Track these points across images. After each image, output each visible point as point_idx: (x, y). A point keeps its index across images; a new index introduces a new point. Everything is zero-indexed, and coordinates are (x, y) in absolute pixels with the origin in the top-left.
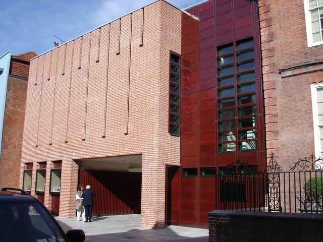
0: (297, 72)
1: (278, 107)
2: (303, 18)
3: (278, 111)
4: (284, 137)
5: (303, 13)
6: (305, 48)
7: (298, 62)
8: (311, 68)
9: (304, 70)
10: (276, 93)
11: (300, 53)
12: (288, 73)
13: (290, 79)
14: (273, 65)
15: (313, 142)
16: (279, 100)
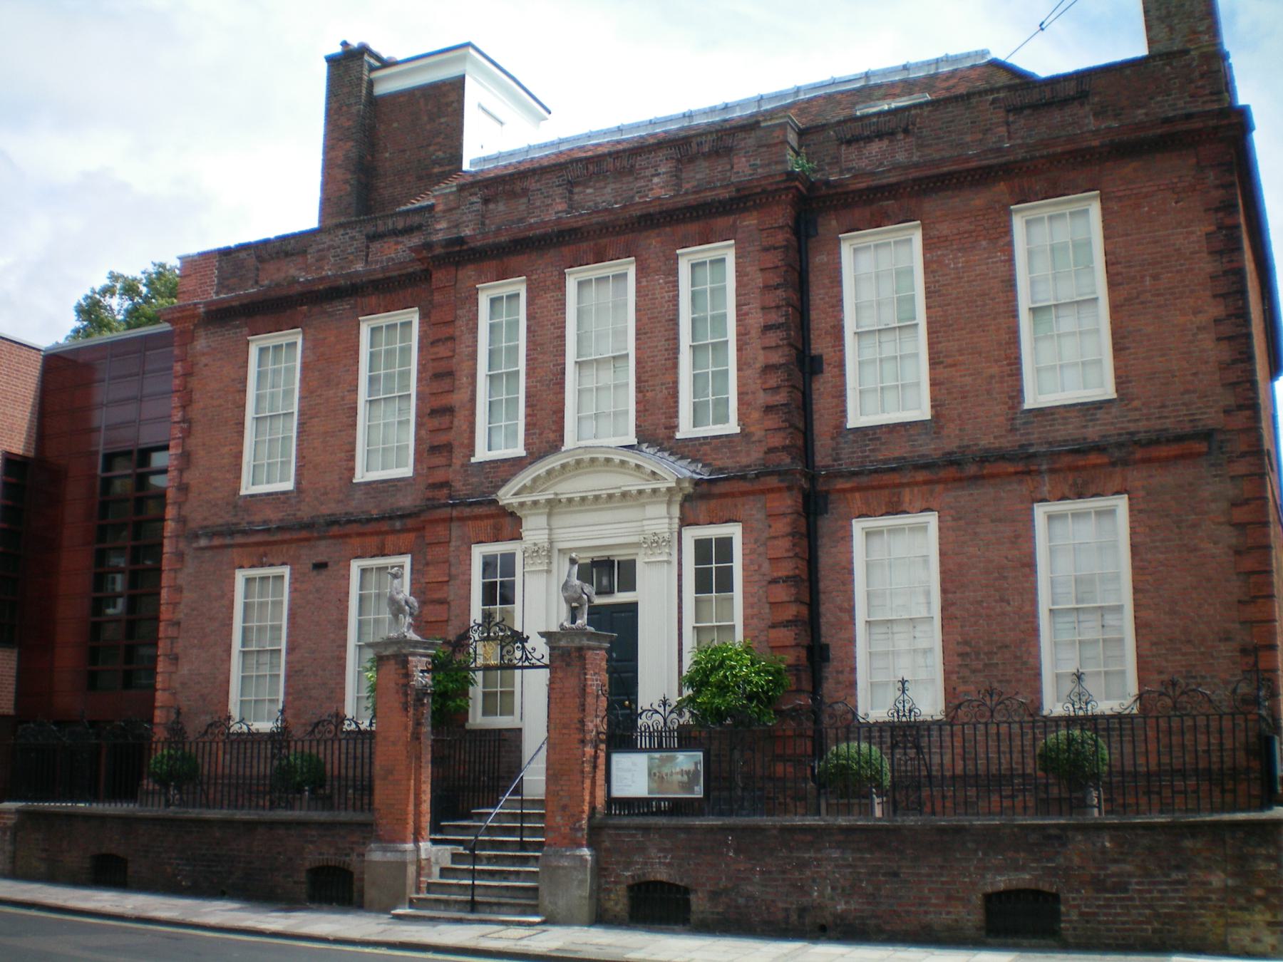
0: (217, 542)
1: (182, 606)
2: (241, 433)
3: (181, 616)
4: (184, 670)
5: (242, 424)
6: (235, 495)
7: (220, 521)
8: (240, 539)
9: (228, 541)
10: (182, 579)
11: (228, 504)
12: (203, 542)
13: (208, 554)
14: (182, 520)
15: (228, 682)
16: (186, 593)
